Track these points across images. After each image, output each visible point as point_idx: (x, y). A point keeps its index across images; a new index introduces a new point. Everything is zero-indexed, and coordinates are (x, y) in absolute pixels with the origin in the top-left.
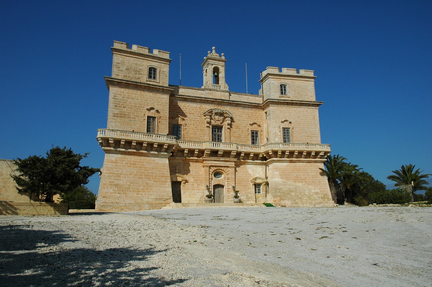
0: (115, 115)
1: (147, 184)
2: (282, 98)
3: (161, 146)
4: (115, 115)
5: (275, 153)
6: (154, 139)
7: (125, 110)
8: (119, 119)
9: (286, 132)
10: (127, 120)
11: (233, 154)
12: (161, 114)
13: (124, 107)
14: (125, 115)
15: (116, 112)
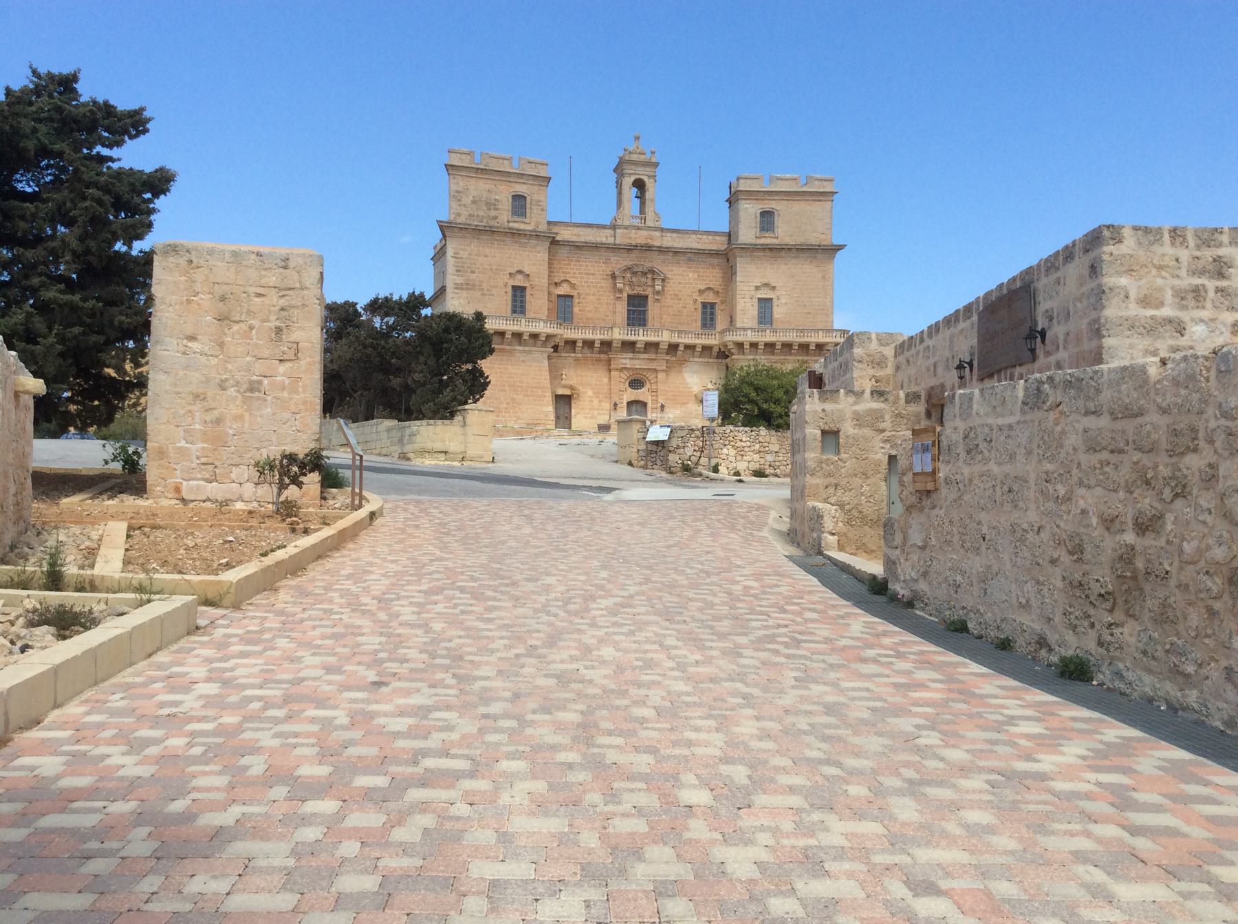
0: (458, 287)
1: (513, 399)
2: (763, 241)
3: (535, 336)
4: (458, 287)
5: (740, 345)
6: (524, 326)
7: (473, 276)
8: (464, 293)
9: (765, 305)
10: (478, 294)
11: (664, 346)
12: (535, 282)
13: (473, 272)
14: (474, 285)
15: (460, 280)
